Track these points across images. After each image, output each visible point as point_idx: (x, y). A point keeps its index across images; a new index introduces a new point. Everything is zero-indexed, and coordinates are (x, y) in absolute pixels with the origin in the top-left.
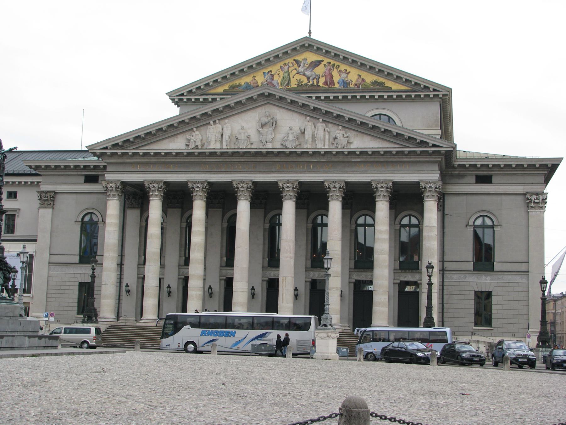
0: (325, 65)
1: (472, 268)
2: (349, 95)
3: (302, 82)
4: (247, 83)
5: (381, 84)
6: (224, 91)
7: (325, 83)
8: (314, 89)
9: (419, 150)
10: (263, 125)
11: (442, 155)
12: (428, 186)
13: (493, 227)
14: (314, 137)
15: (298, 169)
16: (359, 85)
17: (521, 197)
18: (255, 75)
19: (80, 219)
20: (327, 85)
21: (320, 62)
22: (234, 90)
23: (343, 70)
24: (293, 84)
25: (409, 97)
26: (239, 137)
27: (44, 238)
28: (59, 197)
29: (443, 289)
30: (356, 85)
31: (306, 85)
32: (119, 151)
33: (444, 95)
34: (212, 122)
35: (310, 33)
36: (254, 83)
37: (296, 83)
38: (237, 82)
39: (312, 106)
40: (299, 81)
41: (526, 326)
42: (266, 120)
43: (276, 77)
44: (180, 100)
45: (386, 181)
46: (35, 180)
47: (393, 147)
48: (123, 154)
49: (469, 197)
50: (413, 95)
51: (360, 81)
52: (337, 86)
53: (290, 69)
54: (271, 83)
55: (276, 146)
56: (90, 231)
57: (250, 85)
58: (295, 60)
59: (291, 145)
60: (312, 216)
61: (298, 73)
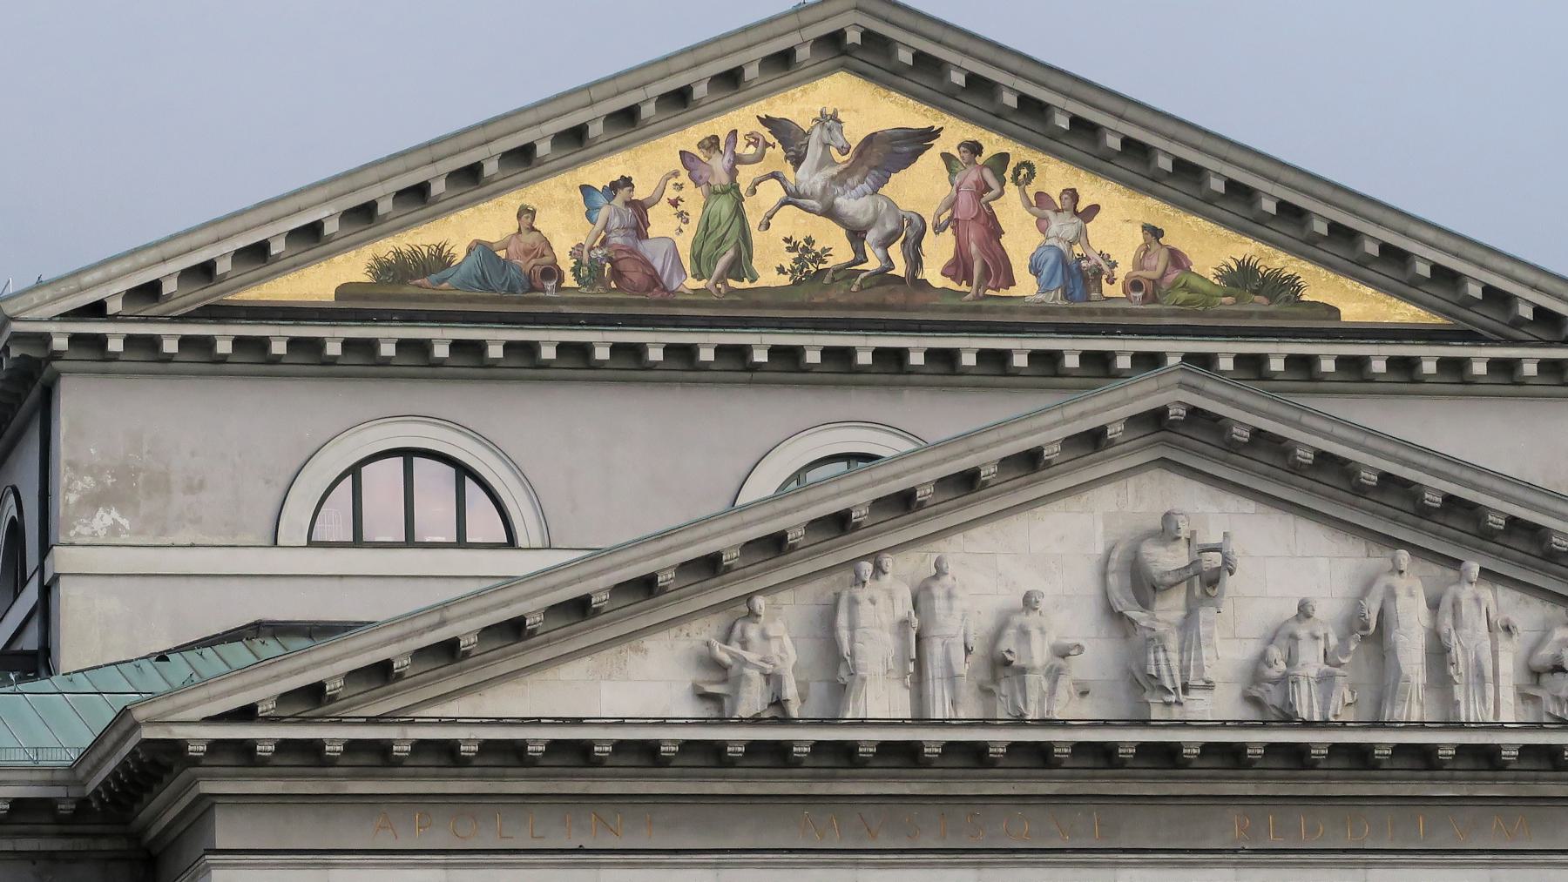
0: (947, 157)
4: (483, 249)
5: (1280, 287)
6: (343, 291)
7: (959, 267)
16: (1155, 283)
18: (530, 202)
20: (967, 276)
21: (923, 139)
22: (409, 290)
23: (1055, 192)
25: (1454, 368)
30: (1136, 285)
31: (846, 273)
36: (527, 253)
37: (788, 260)
38: (421, 238)
40: (804, 251)
43: (661, 222)
44: (75, 339)
51: (1158, 262)
52: (1025, 286)
53: (746, 175)
54: (633, 252)
55: (1214, 707)
57: (505, 264)
58: (767, 121)
61: (793, 198)
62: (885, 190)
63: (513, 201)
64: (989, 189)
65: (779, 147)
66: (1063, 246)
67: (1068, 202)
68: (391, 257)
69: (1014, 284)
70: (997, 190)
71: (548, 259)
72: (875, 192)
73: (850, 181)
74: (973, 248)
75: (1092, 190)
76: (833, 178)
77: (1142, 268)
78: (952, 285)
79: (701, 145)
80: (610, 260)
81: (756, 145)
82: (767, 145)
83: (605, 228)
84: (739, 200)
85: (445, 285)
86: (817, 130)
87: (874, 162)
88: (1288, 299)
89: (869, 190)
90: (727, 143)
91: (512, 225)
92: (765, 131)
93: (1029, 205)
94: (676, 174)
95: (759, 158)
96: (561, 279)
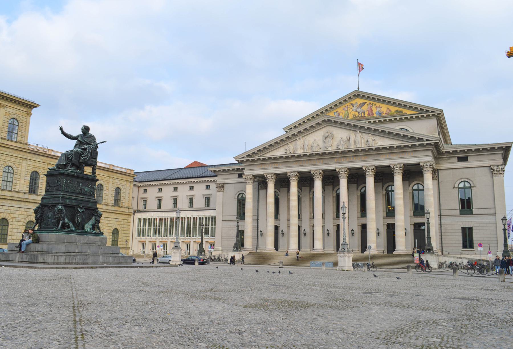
1: (459, 213)
2: (382, 120)
5: (400, 112)
7: (369, 114)
8: (362, 118)
9: (417, 143)
10: (326, 138)
11: (433, 145)
12: (425, 165)
13: (470, 187)
14: (355, 142)
15: (347, 161)
17: (488, 168)
19: (236, 197)
24: (351, 117)
25: (417, 117)
26: (313, 145)
27: (219, 208)
28: (226, 185)
29: (441, 227)
31: (358, 116)
32: (250, 159)
33: (438, 114)
34: (298, 139)
35: (358, 88)
39: (353, 124)
41: (496, 248)
42: (327, 134)
43: (341, 114)
45: (399, 164)
46: (215, 178)
47: (402, 144)
48: (253, 160)
49: (454, 170)
50: (420, 116)
51: (388, 111)
52: (375, 115)
56: (241, 203)
59: (342, 148)
60: (360, 188)
61: (353, 110)
75: (381, 105)
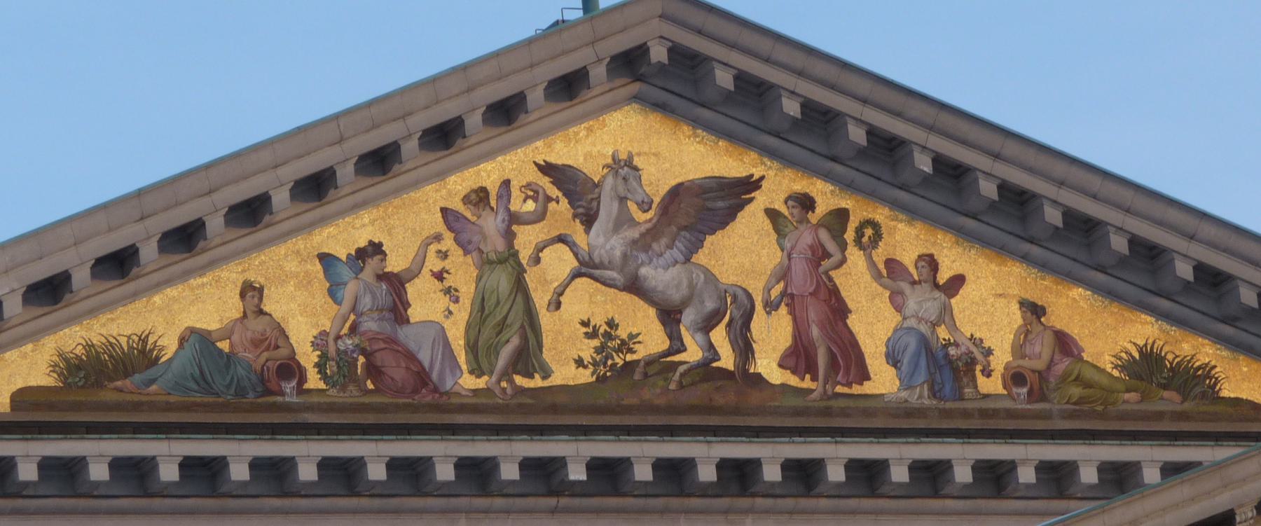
0: (772, 214)
3: (625, 347)
4: (198, 340)
5: (1193, 381)
6: (21, 398)
16: (1042, 375)
18: (257, 278)
21: (739, 192)
22: (108, 396)
23: (908, 258)
24: (566, 364)
30: (1015, 378)
31: (659, 366)
36: (256, 343)
37: (587, 349)
40: (606, 337)
43: (424, 303)
51: (1043, 348)
52: (883, 381)
53: (526, 238)
54: (392, 341)
57: (229, 359)
61: (587, 268)
62: (701, 257)
63: (231, 276)
64: (827, 255)
65: (564, 202)
66: (924, 328)
67: (925, 271)
68: (79, 350)
69: (868, 378)
70: (837, 257)
71: (283, 352)
72: (688, 260)
73: (655, 246)
74: (815, 332)
75: (953, 258)
76: (634, 242)
77: (1023, 357)
78: (793, 381)
79: (466, 200)
80: (364, 352)
81: (535, 199)
82: (549, 199)
83: (353, 309)
84: (519, 273)
85: (154, 388)
86: (610, 181)
87: (683, 221)
88: (1203, 395)
89: (681, 258)
90: (499, 197)
91: (233, 308)
92: (545, 182)
93: (877, 276)
94: (438, 238)
95: (539, 217)
96: (303, 379)
